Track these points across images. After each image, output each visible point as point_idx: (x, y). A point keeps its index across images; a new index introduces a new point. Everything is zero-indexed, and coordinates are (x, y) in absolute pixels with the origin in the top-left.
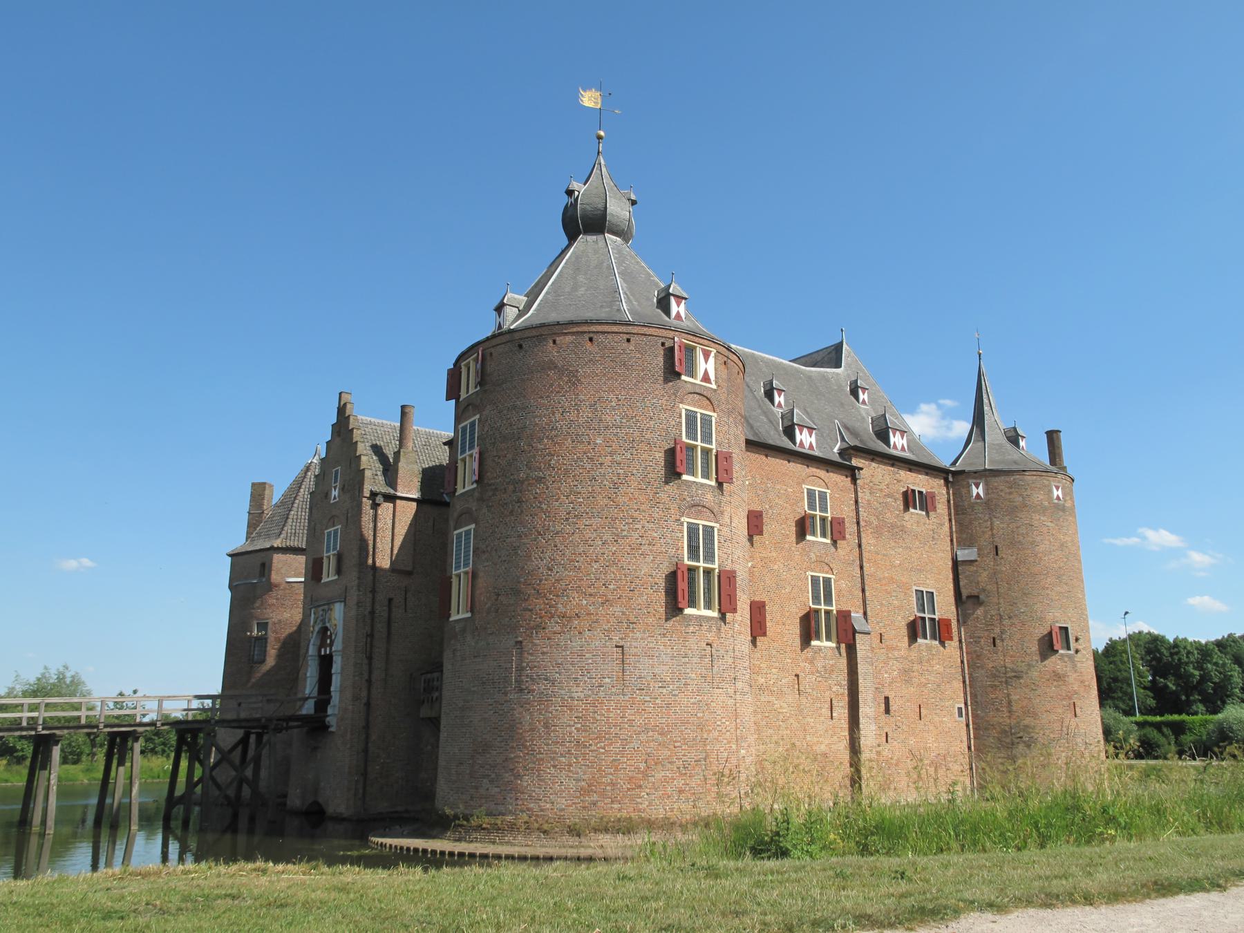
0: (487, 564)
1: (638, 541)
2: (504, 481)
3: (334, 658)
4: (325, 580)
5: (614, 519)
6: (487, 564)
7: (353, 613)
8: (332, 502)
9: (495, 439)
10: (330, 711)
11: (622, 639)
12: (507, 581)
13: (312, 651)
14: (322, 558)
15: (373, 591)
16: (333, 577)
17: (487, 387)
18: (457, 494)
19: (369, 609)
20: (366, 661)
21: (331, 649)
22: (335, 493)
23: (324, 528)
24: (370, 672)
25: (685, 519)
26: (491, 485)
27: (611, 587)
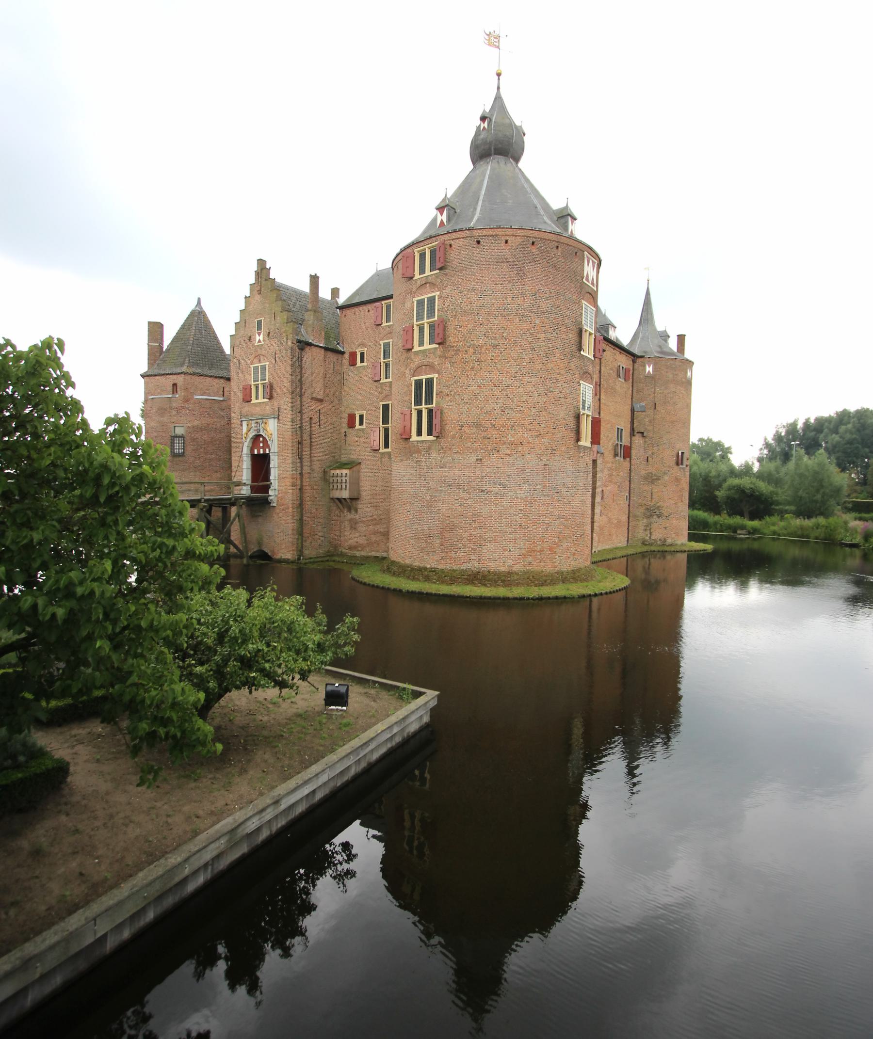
0: (451, 404)
1: (558, 396)
2: (466, 345)
3: (271, 457)
4: (254, 401)
5: (546, 379)
6: (451, 404)
7: (288, 426)
8: (256, 344)
9: (456, 312)
10: (271, 493)
11: (548, 460)
12: (469, 417)
13: (246, 450)
14: (251, 386)
15: (301, 412)
16: (261, 400)
17: (447, 271)
18: (413, 350)
19: (299, 425)
20: (298, 460)
21: (269, 450)
22: (259, 338)
23: (249, 363)
24: (302, 468)
25: (581, 382)
26: (453, 347)
27: (542, 425)
